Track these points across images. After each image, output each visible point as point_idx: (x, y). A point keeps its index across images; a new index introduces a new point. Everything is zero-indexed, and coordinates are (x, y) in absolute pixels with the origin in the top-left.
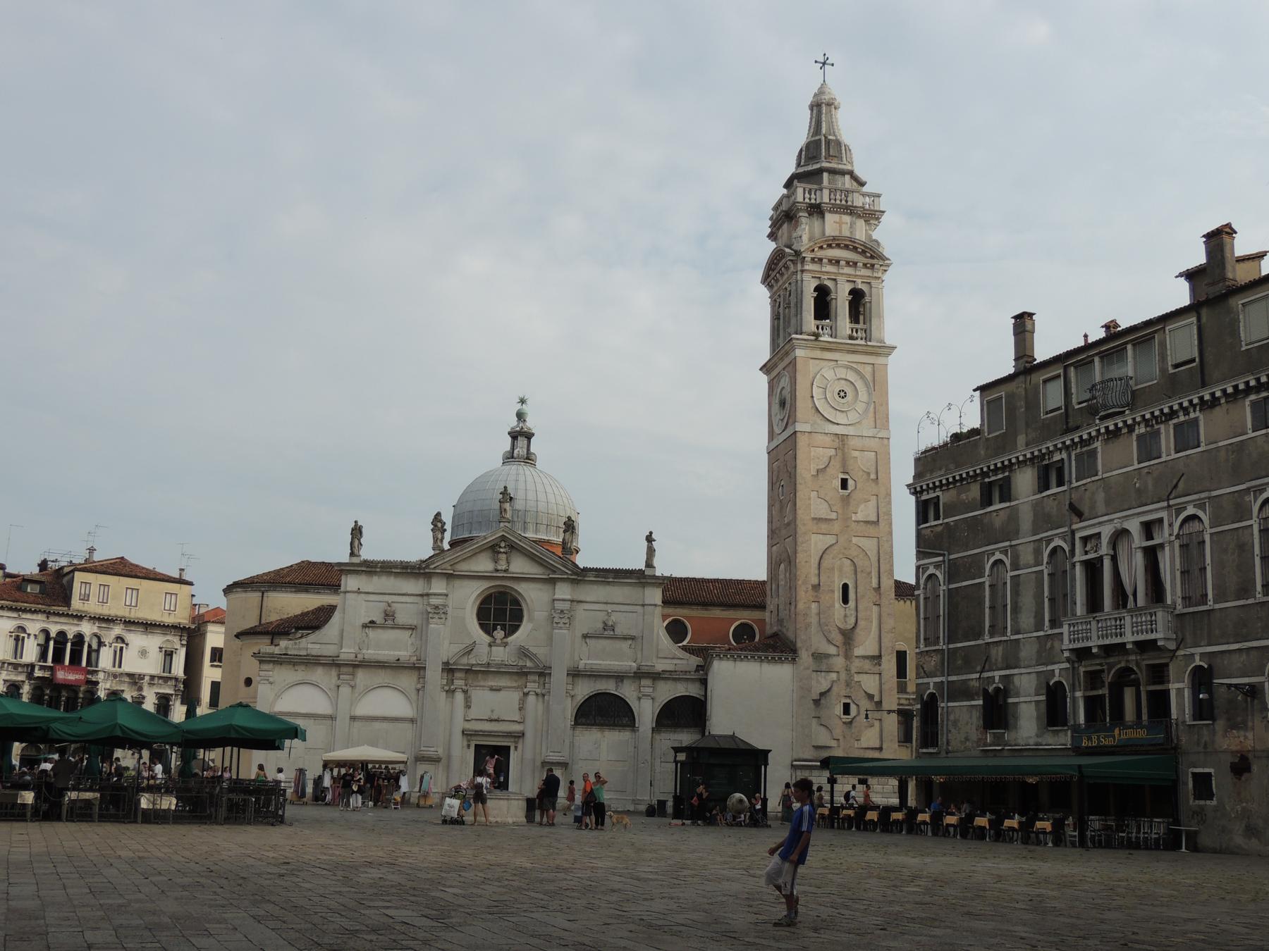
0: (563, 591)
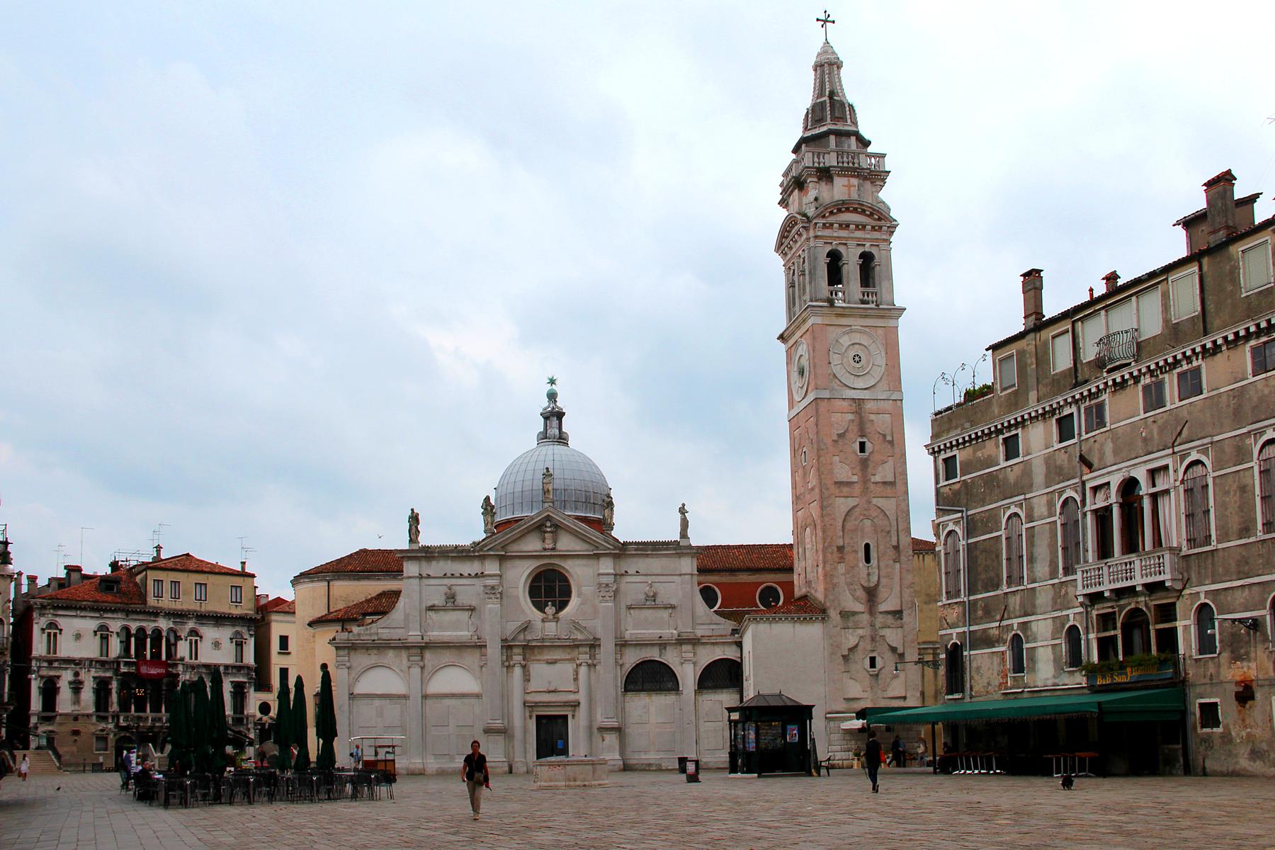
0: (606, 566)
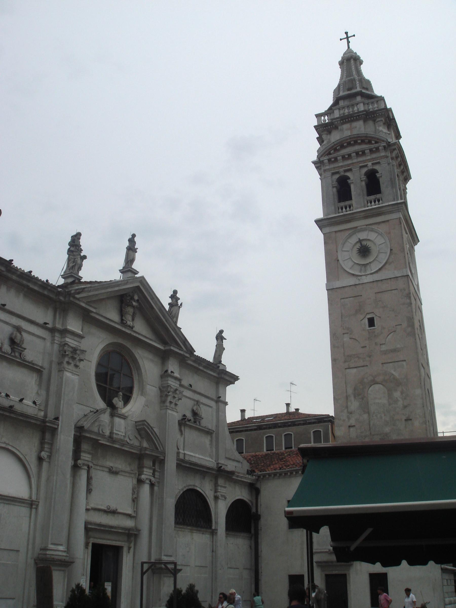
0: (173, 366)
